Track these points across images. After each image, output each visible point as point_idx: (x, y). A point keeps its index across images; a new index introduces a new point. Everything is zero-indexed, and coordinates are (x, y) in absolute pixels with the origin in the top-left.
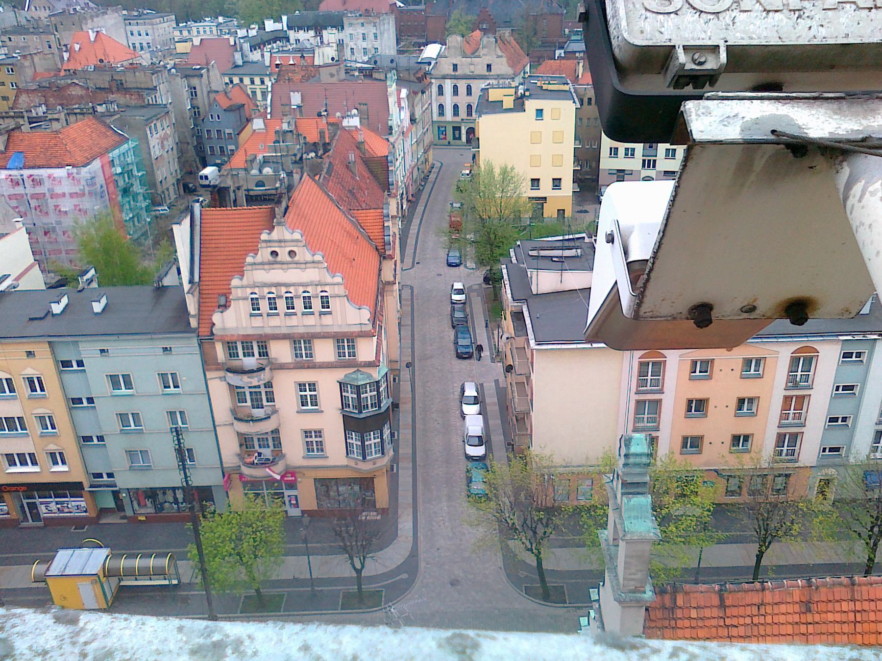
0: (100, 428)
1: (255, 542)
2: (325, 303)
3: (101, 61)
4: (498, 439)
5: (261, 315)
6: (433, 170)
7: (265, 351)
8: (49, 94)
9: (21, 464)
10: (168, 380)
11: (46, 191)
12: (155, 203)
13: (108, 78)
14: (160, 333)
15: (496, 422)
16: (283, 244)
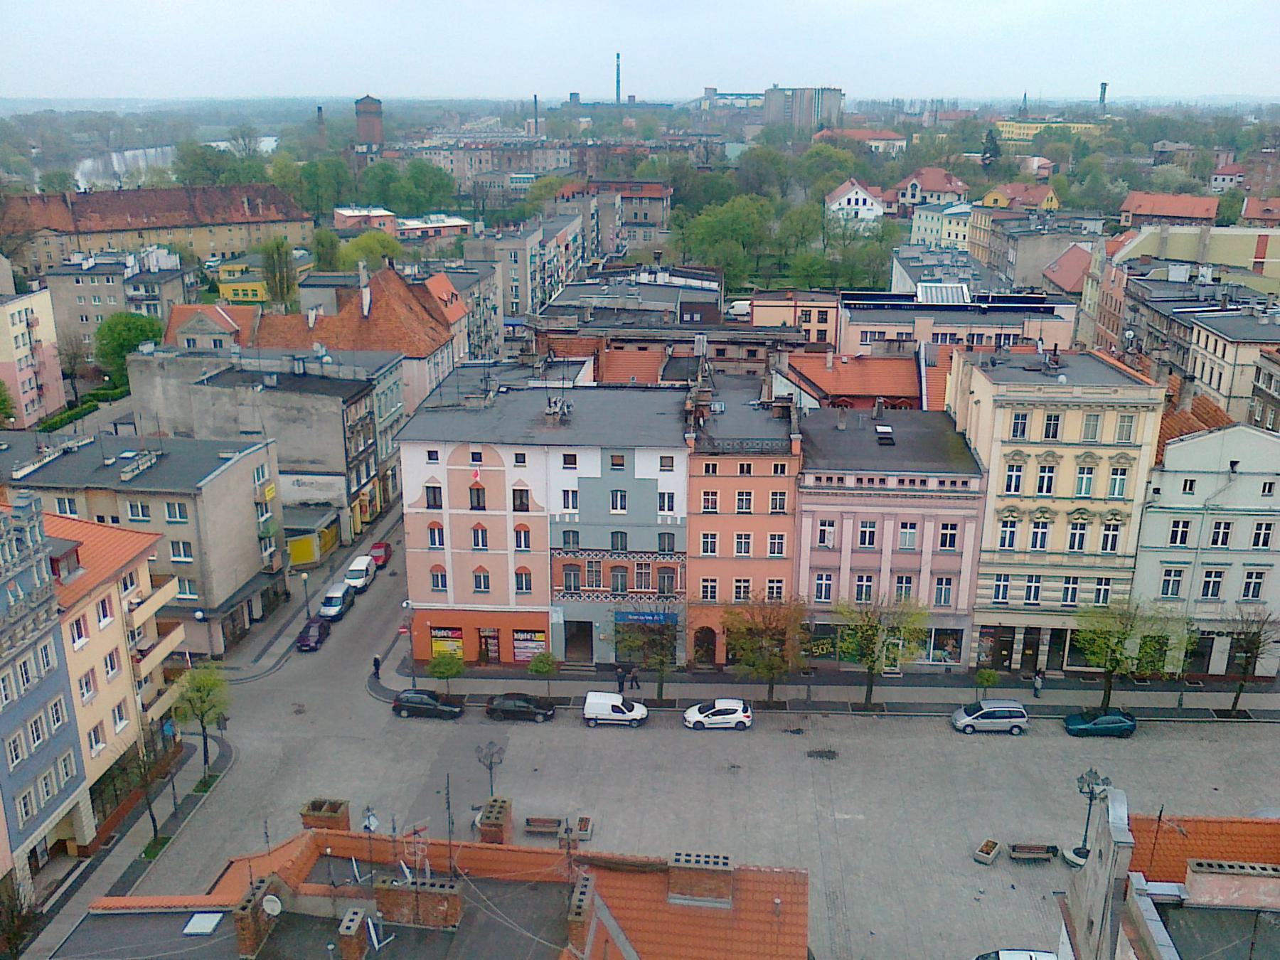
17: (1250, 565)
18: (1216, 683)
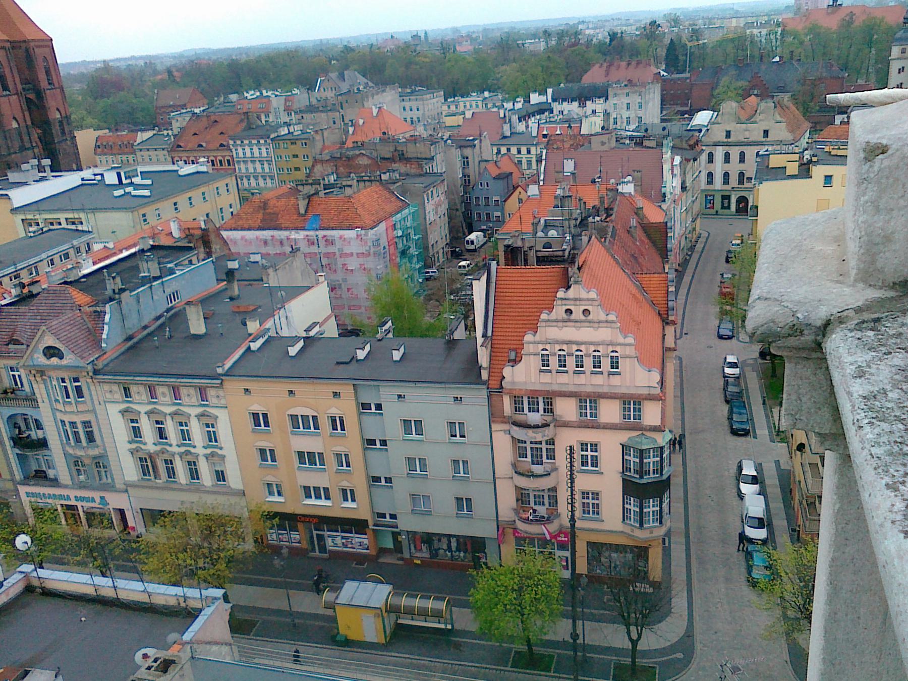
1: (536, 594)
2: (615, 364)
3: (384, 133)
4: (781, 523)
5: (550, 371)
6: (700, 239)
7: (550, 407)
8: (339, 164)
9: (316, 498)
10: (456, 429)
11: (336, 251)
12: (427, 266)
13: (392, 149)
14: (453, 383)
15: (778, 506)
16: (578, 302)
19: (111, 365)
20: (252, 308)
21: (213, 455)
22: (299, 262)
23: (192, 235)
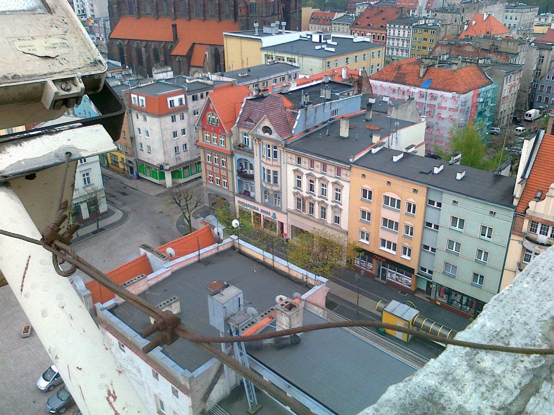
0: (436, 244)
3: (488, 33)
8: (453, 49)
9: (387, 247)
10: (486, 231)
12: (494, 125)
13: (491, 44)
14: (492, 202)
17: (83, 171)
18: (87, 222)
19: (294, 143)
20: (378, 128)
21: (336, 207)
22: (411, 107)
23: (353, 79)
